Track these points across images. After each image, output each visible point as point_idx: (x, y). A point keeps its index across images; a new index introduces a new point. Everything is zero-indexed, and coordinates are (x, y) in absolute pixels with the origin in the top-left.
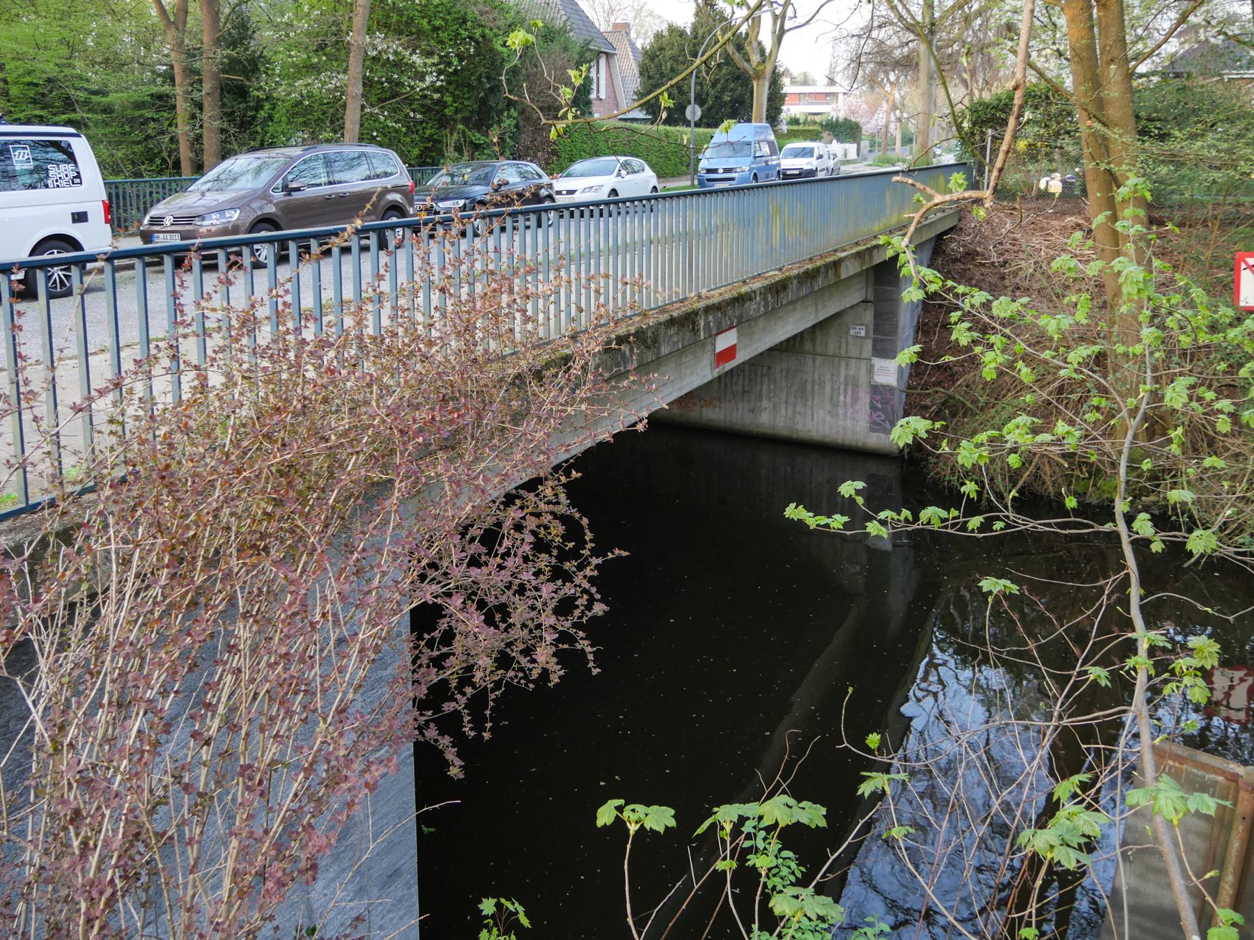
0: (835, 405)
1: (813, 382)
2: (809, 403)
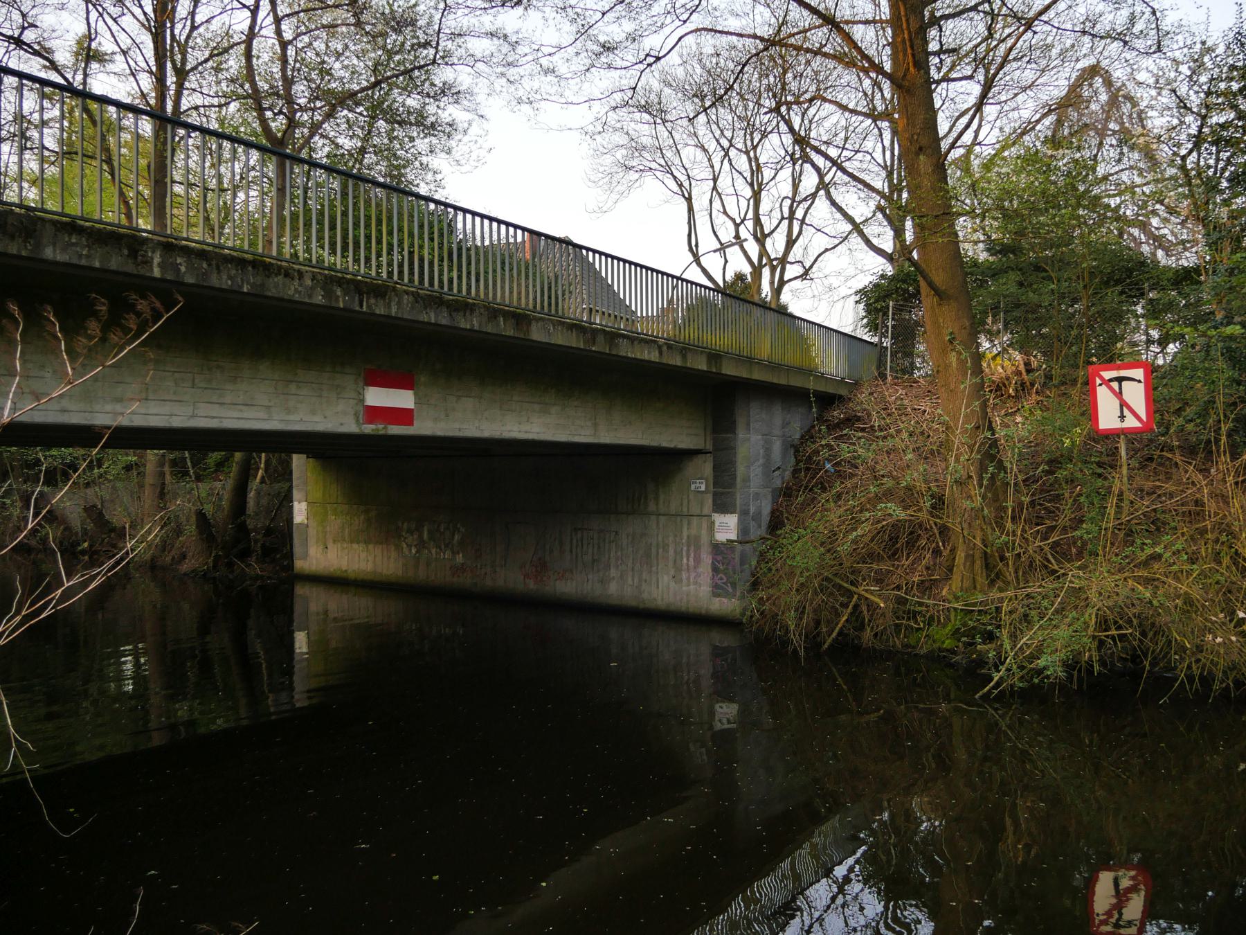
0: (678, 570)
1: (658, 545)
2: (654, 569)
